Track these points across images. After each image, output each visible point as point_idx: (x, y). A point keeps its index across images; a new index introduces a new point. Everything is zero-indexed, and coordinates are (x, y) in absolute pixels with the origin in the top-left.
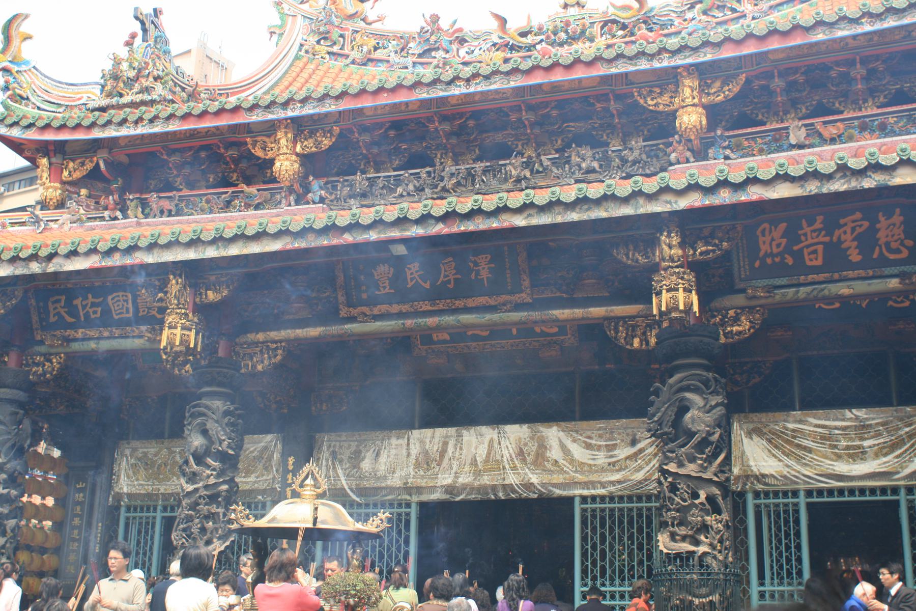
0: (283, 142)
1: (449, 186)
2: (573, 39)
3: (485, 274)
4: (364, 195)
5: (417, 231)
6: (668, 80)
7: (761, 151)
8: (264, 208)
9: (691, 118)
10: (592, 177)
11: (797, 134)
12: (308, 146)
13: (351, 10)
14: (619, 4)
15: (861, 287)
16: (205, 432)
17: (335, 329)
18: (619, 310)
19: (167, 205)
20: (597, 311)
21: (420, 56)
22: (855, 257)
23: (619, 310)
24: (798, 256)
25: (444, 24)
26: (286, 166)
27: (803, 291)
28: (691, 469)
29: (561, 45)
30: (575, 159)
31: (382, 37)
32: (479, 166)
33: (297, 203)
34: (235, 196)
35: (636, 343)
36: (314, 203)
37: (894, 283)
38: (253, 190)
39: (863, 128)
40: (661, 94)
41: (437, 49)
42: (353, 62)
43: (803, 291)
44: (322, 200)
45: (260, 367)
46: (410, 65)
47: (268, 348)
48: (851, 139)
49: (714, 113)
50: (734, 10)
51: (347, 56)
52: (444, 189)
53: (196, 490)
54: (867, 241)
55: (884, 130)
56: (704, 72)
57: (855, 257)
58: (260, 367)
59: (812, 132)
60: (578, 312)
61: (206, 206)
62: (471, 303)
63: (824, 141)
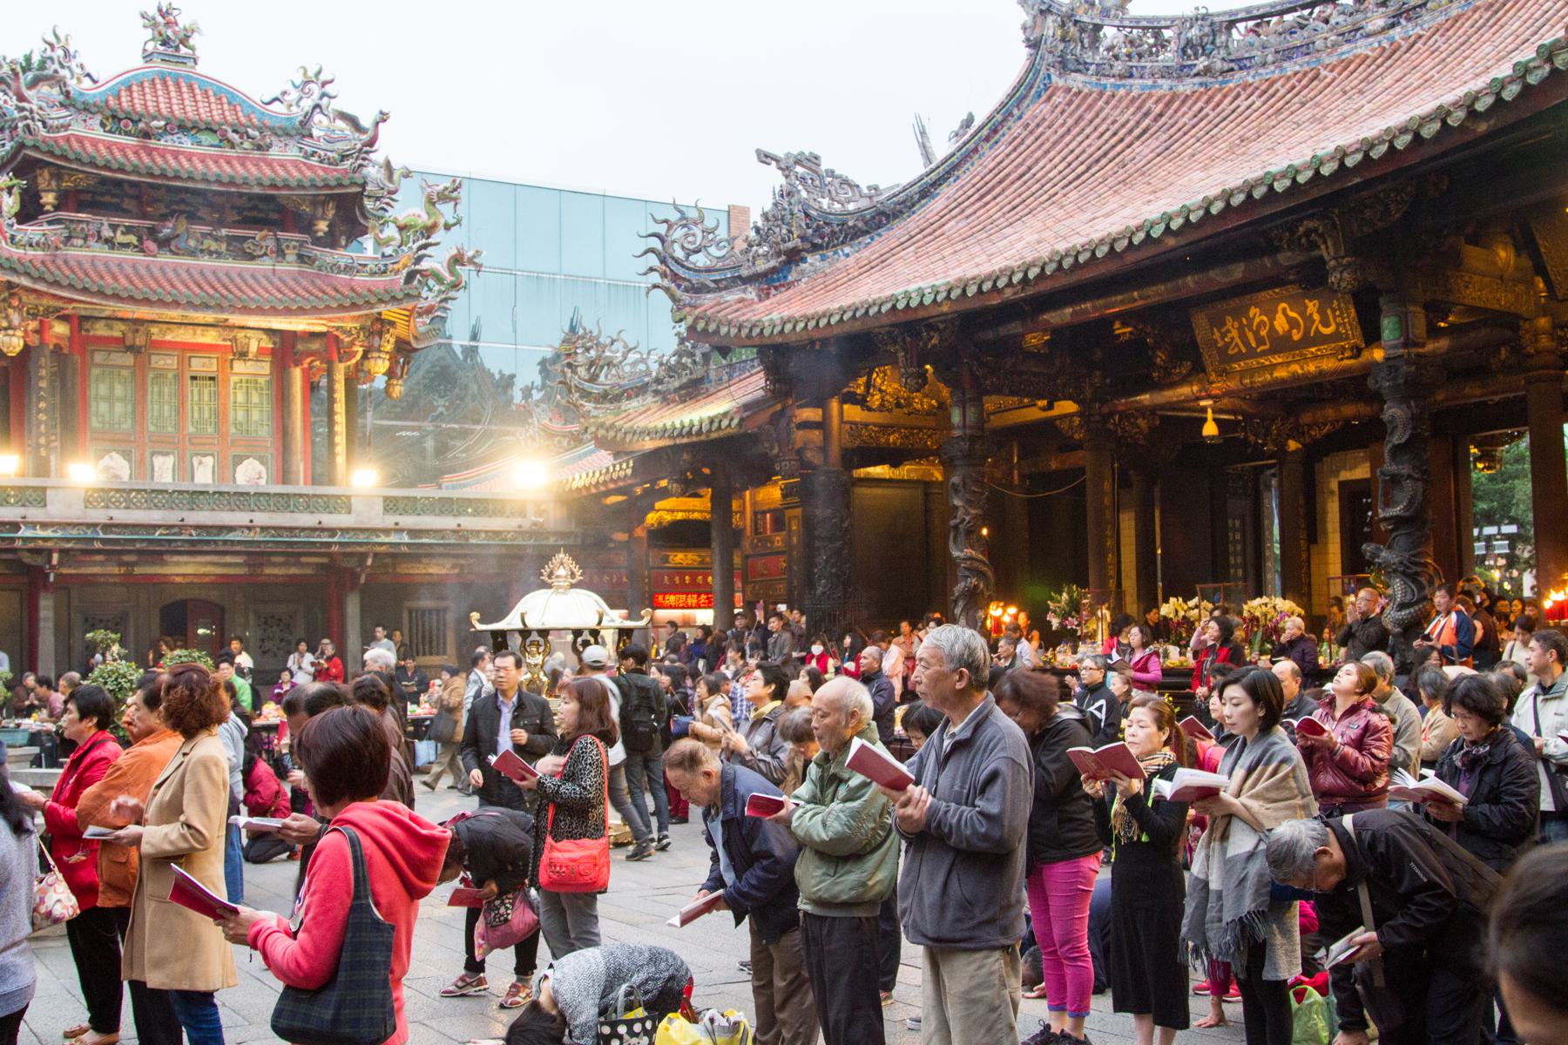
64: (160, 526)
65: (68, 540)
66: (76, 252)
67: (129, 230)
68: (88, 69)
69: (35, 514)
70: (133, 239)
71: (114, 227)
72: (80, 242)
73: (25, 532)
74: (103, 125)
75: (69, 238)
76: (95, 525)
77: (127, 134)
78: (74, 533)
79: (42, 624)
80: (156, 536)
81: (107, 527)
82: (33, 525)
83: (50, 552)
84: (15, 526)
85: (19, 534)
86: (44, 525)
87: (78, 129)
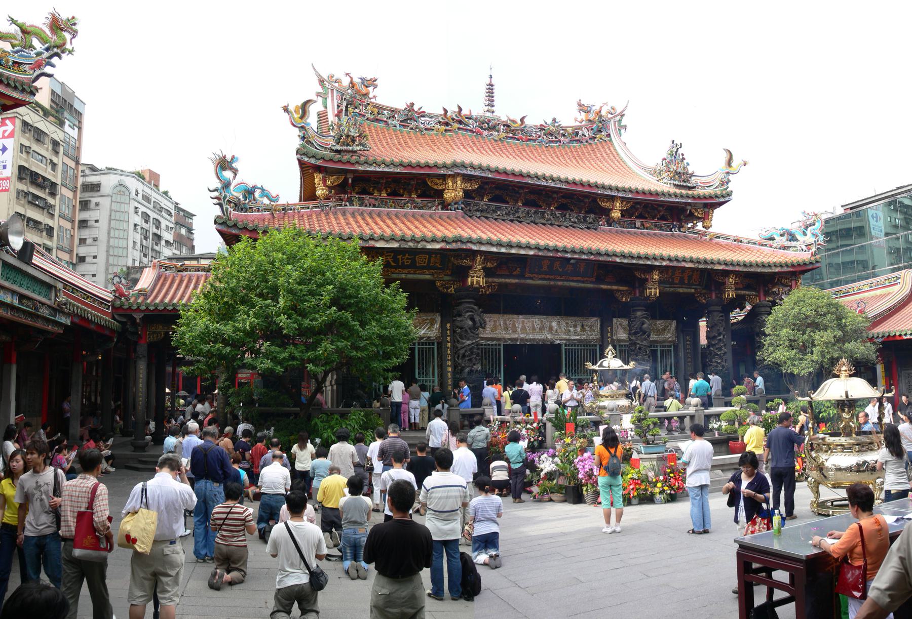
3: (582, 269)
5: (584, 257)
6: (612, 199)
9: (616, 214)
11: (638, 224)
15: (686, 290)
16: (472, 319)
17: (523, 281)
20: (615, 287)
22: (686, 282)
23: (621, 288)
24: (673, 279)
30: (567, 216)
32: (533, 210)
39: (656, 226)
49: (624, 213)
54: (690, 277)
55: (661, 228)
57: (686, 282)
59: (642, 224)
60: (609, 287)
62: (575, 279)
63: (644, 228)
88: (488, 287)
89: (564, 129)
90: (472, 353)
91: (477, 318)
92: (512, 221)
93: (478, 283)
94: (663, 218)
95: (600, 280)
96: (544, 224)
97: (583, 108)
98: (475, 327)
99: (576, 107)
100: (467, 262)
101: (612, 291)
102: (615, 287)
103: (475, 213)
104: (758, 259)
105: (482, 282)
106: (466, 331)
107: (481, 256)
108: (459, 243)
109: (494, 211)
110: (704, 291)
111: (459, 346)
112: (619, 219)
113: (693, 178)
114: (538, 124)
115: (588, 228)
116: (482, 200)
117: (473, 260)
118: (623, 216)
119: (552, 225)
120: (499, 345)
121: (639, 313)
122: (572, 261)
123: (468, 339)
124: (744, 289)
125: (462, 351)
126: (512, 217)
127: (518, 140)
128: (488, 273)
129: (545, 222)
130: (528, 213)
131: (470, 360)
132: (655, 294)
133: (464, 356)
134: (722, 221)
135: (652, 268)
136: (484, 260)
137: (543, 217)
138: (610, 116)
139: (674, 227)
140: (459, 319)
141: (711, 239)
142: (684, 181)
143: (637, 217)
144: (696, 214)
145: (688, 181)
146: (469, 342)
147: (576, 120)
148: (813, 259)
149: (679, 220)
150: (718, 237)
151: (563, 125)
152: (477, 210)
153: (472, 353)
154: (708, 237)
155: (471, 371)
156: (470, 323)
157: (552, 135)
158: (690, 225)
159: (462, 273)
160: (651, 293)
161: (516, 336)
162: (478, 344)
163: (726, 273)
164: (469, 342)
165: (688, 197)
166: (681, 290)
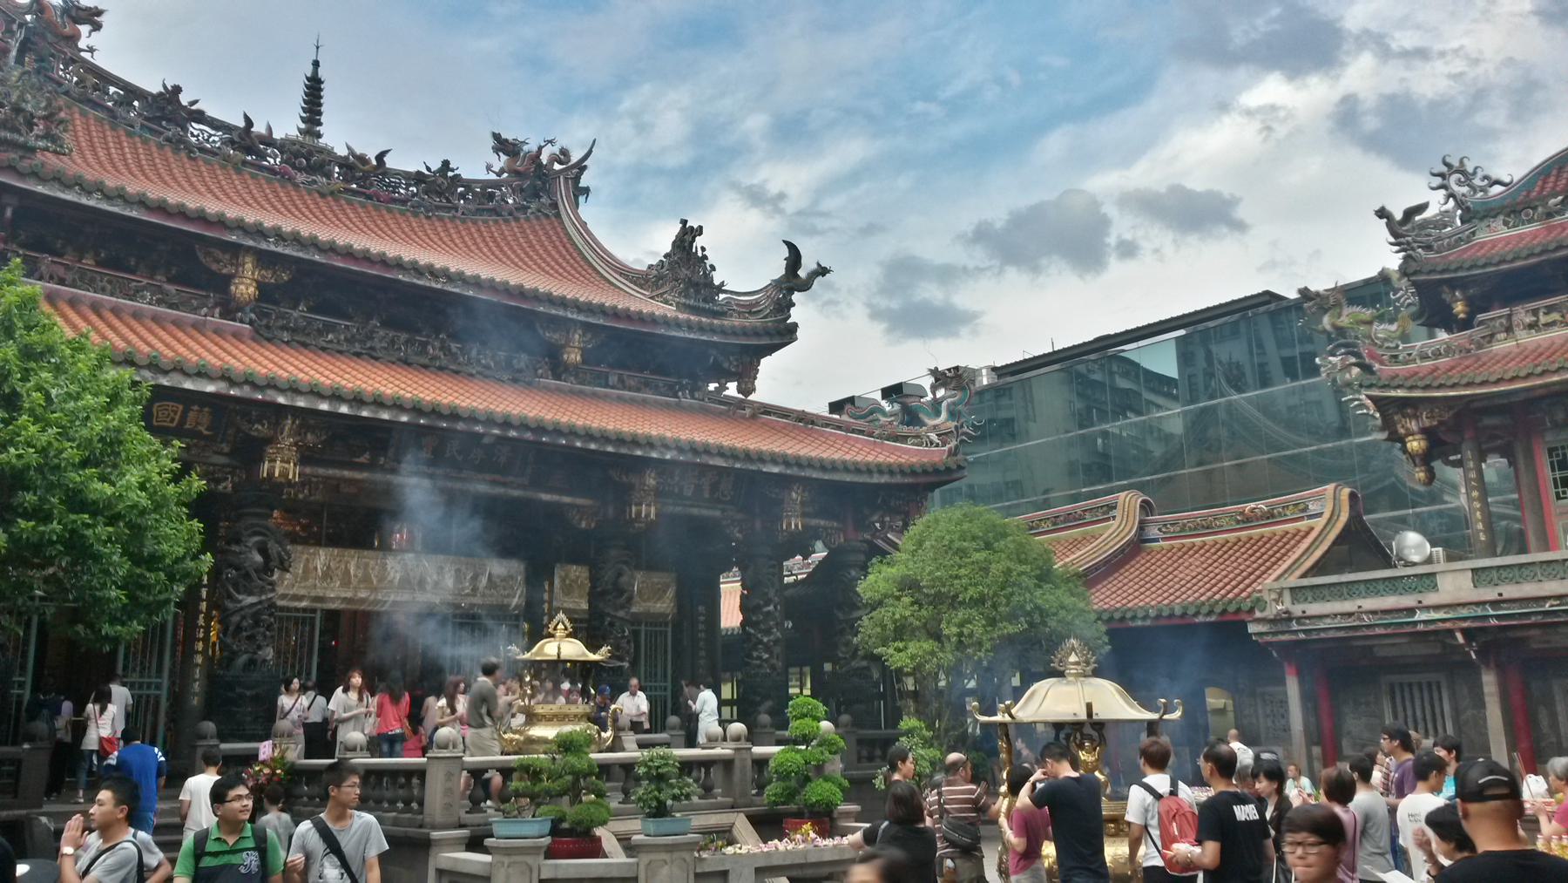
0: (249, 266)
1: (378, 346)
2: (311, 169)
3: (503, 460)
4: (294, 331)
7: (589, 384)
8: (177, 309)
10: (488, 372)
11: (613, 379)
12: (268, 276)
13: (67, 30)
14: (358, 151)
15: (705, 512)
16: (263, 551)
18: (580, 501)
19: (61, 271)
20: (567, 499)
21: (147, 119)
22: (707, 496)
23: (580, 501)
25: (184, 99)
26: (245, 289)
27: (678, 509)
28: (621, 614)
29: (300, 170)
30: (474, 353)
31: (106, 78)
32: (404, 336)
33: (222, 316)
34: (144, 288)
35: (583, 525)
36: (241, 321)
37: (718, 513)
38: (171, 288)
40: (555, 331)
41: (169, 120)
42: (67, 93)
43: (678, 509)
44: (251, 323)
45: (301, 496)
46: (137, 128)
47: (310, 482)
48: (638, 390)
50: (448, 201)
51: (60, 84)
52: (372, 348)
53: (260, 602)
54: (714, 487)
55: (656, 390)
56: (587, 327)
58: (301, 496)
59: (621, 380)
60: (555, 498)
61: (109, 287)
63: (624, 388)
64: (1549, 598)
65: (1465, 619)
66: (1502, 346)
67: (1550, 309)
68: (1494, 176)
69: (1431, 598)
70: (1555, 316)
71: (1535, 312)
72: (1503, 335)
73: (1420, 616)
74: (1506, 223)
75: (1492, 335)
76: (1484, 603)
77: (1529, 222)
78: (1464, 612)
79: (1487, 699)
80: (1547, 607)
81: (1495, 604)
82: (1428, 608)
83: (1451, 632)
84: (1411, 611)
85: (1416, 618)
86: (1437, 608)
87: (1483, 236)
88: (303, 484)
89: (469, 184)
90: (257, 623)
91: (274, 548)
92: (358, 355)
93: (284, 474)
94: (661, 370)
95: (537, 483)
96: (425, 367)
97: (502, 145)
98: (267, 569)
99: (491, 142)
100: (260, 429)
101: (559, 505)
102: (567, 499)
103: (278, 333)
104: (847, 457)
105: (293, 472)
106: (247, 576)
107: (294, 418)
108: (247, 388)
109: (320, 333)
110: (739, 516)
111: (230, 605)
112: (576, 366)
113: (722, 296)
114: (412, 169)
115: (515, 381)
116: (295, 307)
117: (277, 423)
118: (584, 361)
119: (441, 368)
120: (314, 611)
121: (613, 553)
122: (486, 440)
123: (250, 594)
124: (816, 516)
125: (235, 619)
126: (357, 347)
127: (369, 197)
128: (306, 457)
129: (426, 361)
130: (393, 342)
131: (251, 638)
132: (648, 515)
133: (239, 628)
134: (779, 380)
135: (645, 462)
136: (301, 426)
137: (424, 352)
138: (557, 167)
139: (682, 388)
140: (235, 548)
141: (753, 416)
142: (705, 300)
143: (611, 366)
144: (726, 365)
145: (713, 301)
146: (251, 600)
147: (489, 168)
148: (952, 464)
149: (693, 377)
150: (769, 413)
151: (466, 175)
152: (283, 328)
153: (257, 623)
154: (748, 412)
155: (252, 663)
156: (258, 558)
157: (440, 194)
158: (712, 387)
159: (251, 451)
160: (639, 513)
161: (349, 595)
162: (272, 605)
163: (784, 481)
164: (251, 600)
165: (713, 330)
166: (695, 511)
